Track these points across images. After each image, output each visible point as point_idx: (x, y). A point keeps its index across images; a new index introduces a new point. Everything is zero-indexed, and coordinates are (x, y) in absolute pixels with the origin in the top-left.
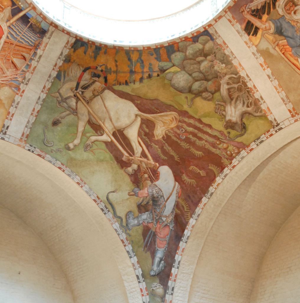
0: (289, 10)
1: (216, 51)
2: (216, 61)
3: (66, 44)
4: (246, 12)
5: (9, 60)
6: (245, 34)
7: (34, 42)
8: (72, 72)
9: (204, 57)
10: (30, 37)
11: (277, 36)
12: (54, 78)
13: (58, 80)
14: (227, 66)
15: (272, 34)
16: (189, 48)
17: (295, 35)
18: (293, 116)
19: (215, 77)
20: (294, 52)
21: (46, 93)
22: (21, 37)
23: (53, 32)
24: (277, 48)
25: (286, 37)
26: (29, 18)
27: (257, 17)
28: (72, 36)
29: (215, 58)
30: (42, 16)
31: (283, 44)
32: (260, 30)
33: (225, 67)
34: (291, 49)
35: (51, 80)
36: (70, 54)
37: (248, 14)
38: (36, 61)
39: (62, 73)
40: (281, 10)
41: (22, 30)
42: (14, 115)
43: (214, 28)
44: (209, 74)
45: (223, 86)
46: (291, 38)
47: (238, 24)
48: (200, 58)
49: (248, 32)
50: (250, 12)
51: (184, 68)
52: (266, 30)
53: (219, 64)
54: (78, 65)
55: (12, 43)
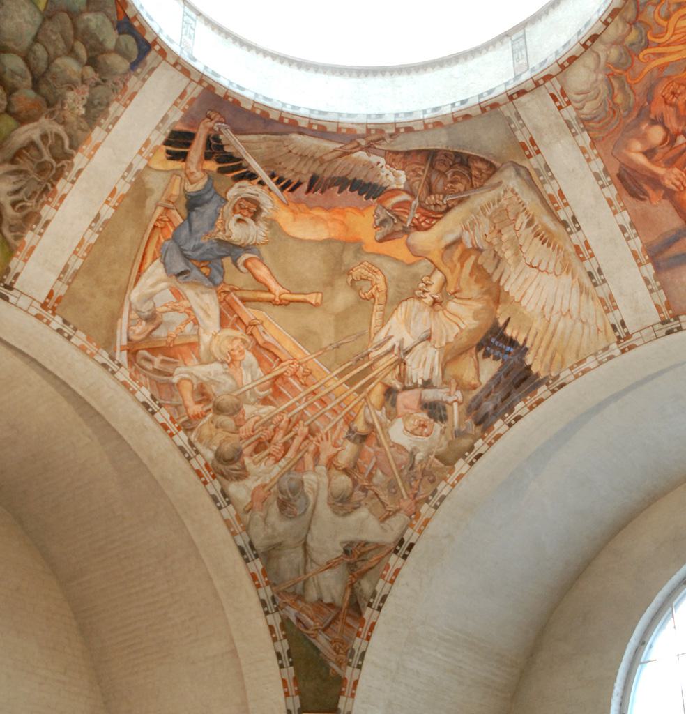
0: (241, 209)
1: (110, 83)
2: (87, 89)
4: (210, 124)
6: (164, 134)
9: (89, 59)
11: (184, 200)
14: (81, 119)
15: (184, 190)
16: (100, 16)
17: (199, 235)
18: (44, 305)
19: (47, 101)
20: (166, 247)
24: (160, 210)
25: (188, 219)
27: (207, 149)
29: (93, 85)
31: (173, 220)
32: (184, 164)
33: (80, 114)
34: (170, 237)
37: (208, 130)
40: (235, 194)
43: (160, 63)
44: (50, 84)
45: (36, 128)
46: (190, 230)
47: (181, 113)
48: (82, 51)
49: (171, 139)
50: (212, 133)
51: (50, 18)
52: (187, 176)
53: (83, 99)
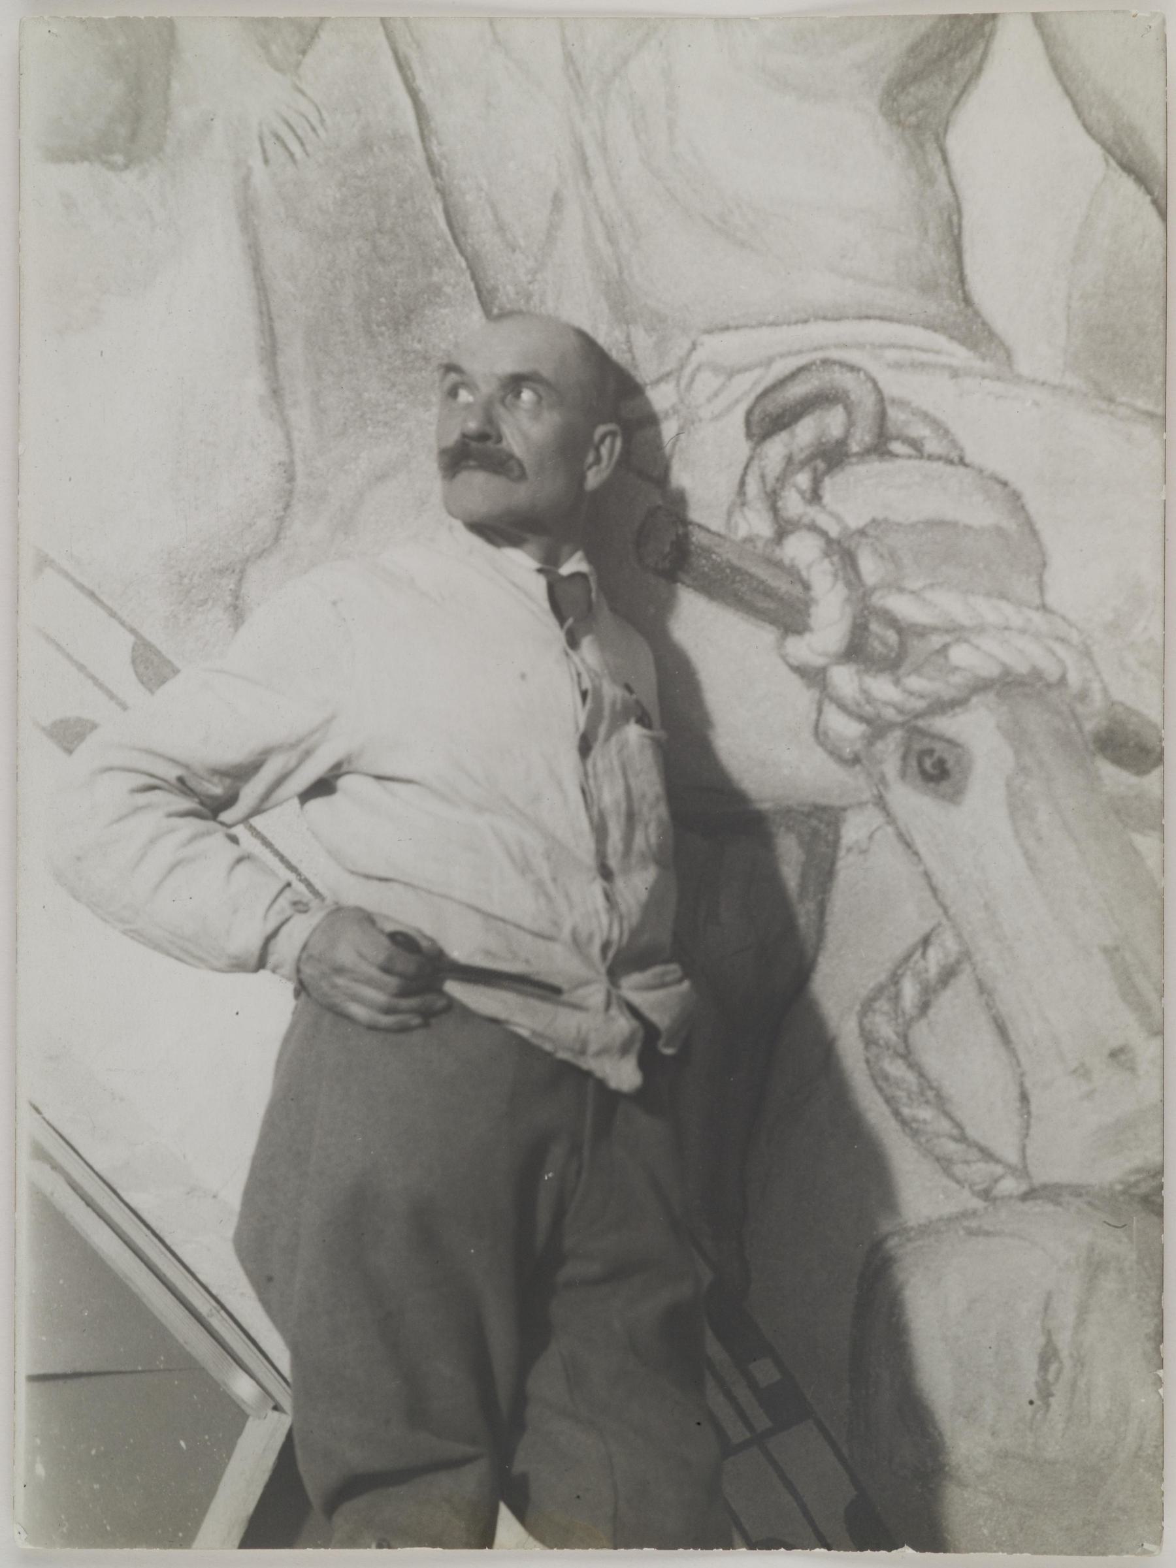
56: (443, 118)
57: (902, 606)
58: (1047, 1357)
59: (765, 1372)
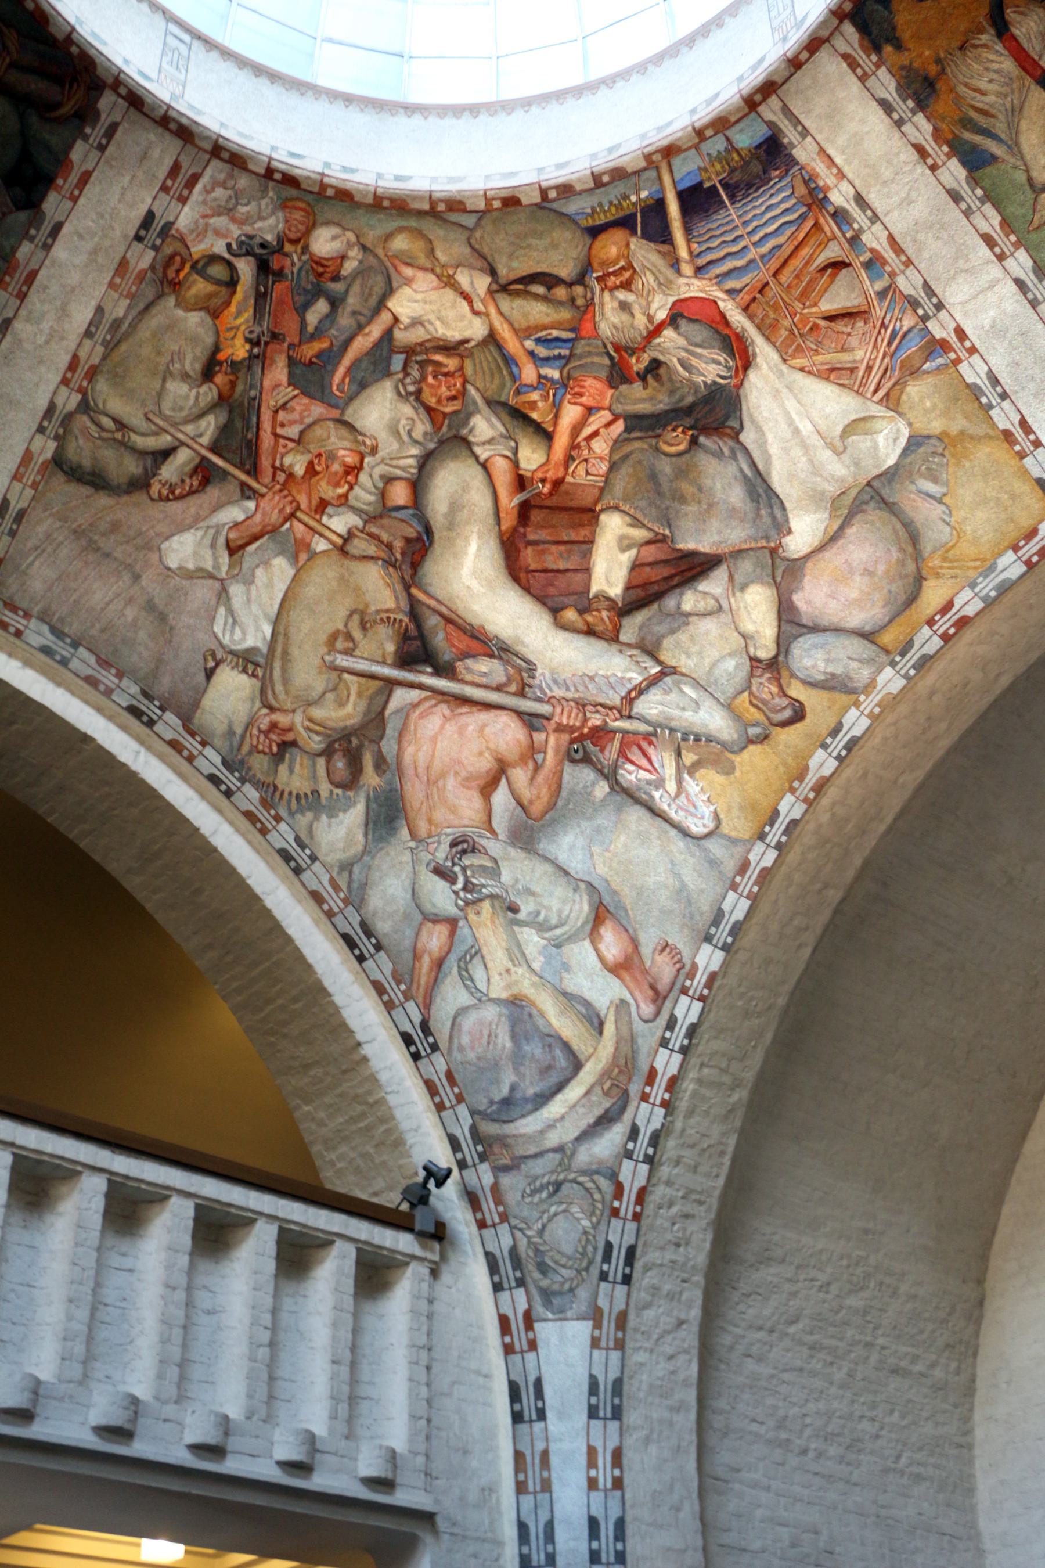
3: (854, 71)
5: (815, 327)
7: (793, 201)
8: (983, 93)
10: (769, 208)
12: (974, 180)
13: (988, 170)
21: (1017, 245)
22: (754, 244)
23: (786, 110)
26: (701, 184)
28: (832, 34)
30: (709, 133)
35: (972, 196)
36: (903, 68)
38: (868, 223)
39: (967, 135)
41: (730, 227)
42: (1030, 421)
54: (962, 48)
55: (759, 285)
56: (405, 787)
57: (474, 881)
58: (489, 1036)
59: (431, 1040)
